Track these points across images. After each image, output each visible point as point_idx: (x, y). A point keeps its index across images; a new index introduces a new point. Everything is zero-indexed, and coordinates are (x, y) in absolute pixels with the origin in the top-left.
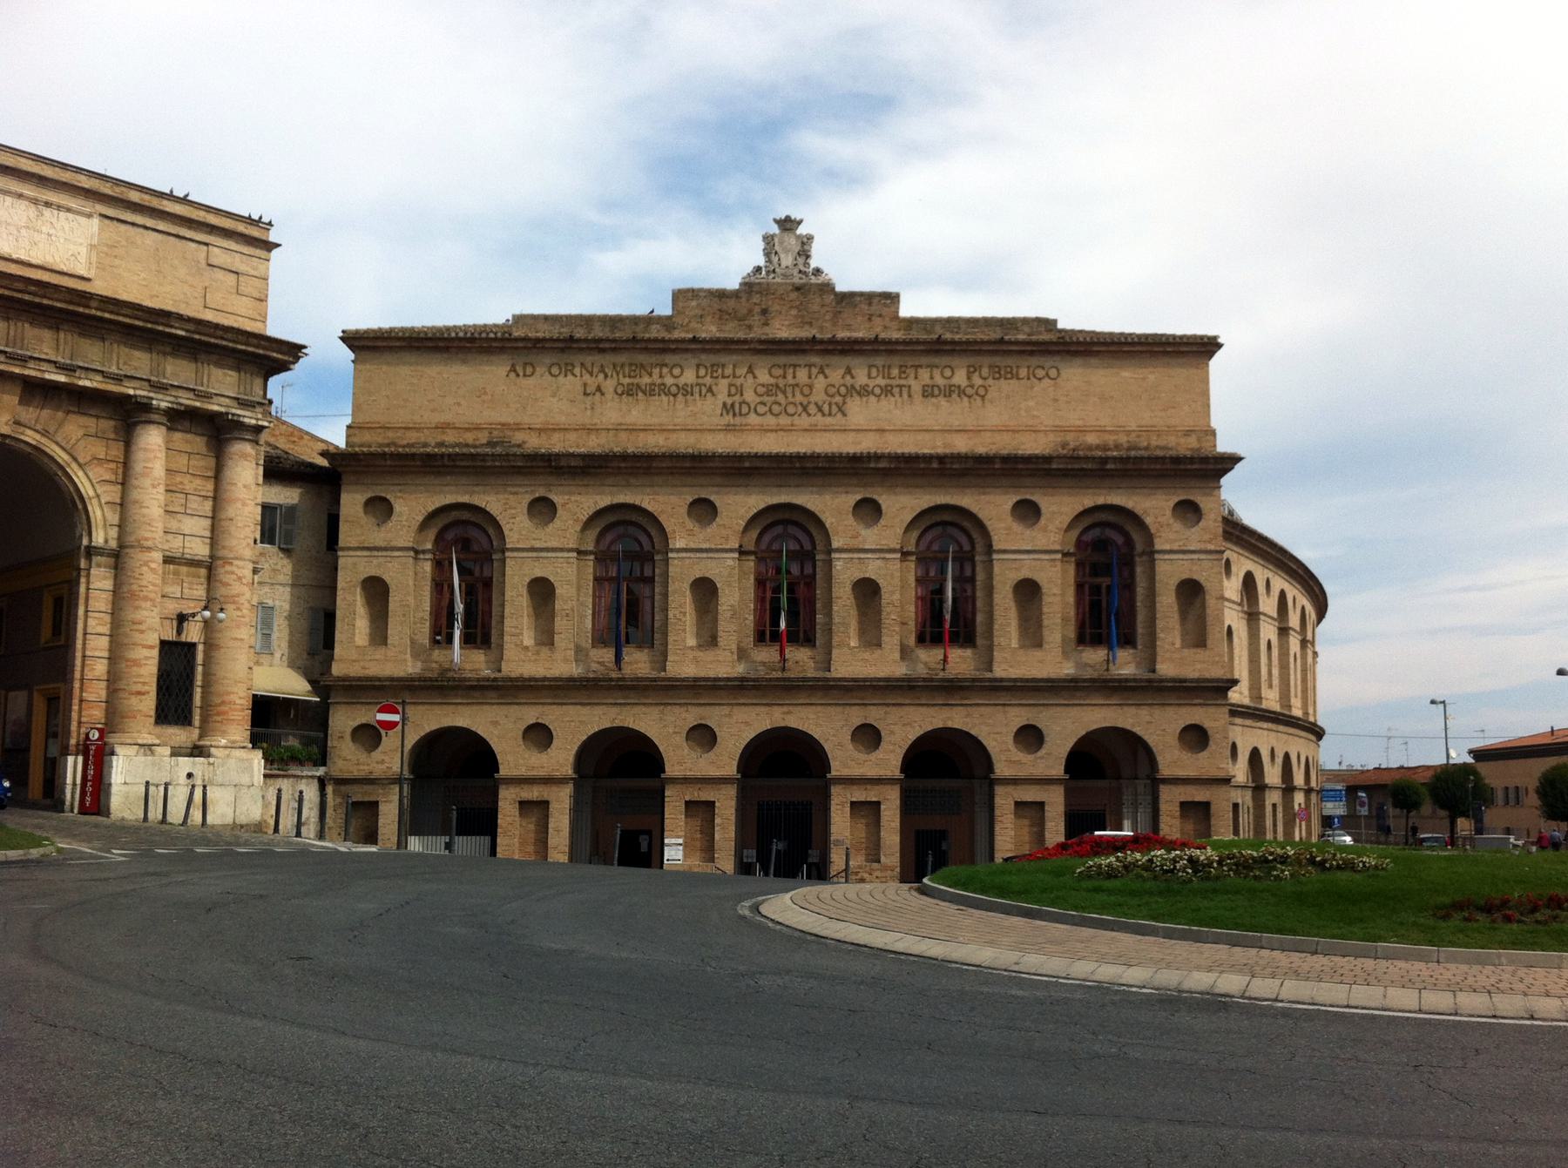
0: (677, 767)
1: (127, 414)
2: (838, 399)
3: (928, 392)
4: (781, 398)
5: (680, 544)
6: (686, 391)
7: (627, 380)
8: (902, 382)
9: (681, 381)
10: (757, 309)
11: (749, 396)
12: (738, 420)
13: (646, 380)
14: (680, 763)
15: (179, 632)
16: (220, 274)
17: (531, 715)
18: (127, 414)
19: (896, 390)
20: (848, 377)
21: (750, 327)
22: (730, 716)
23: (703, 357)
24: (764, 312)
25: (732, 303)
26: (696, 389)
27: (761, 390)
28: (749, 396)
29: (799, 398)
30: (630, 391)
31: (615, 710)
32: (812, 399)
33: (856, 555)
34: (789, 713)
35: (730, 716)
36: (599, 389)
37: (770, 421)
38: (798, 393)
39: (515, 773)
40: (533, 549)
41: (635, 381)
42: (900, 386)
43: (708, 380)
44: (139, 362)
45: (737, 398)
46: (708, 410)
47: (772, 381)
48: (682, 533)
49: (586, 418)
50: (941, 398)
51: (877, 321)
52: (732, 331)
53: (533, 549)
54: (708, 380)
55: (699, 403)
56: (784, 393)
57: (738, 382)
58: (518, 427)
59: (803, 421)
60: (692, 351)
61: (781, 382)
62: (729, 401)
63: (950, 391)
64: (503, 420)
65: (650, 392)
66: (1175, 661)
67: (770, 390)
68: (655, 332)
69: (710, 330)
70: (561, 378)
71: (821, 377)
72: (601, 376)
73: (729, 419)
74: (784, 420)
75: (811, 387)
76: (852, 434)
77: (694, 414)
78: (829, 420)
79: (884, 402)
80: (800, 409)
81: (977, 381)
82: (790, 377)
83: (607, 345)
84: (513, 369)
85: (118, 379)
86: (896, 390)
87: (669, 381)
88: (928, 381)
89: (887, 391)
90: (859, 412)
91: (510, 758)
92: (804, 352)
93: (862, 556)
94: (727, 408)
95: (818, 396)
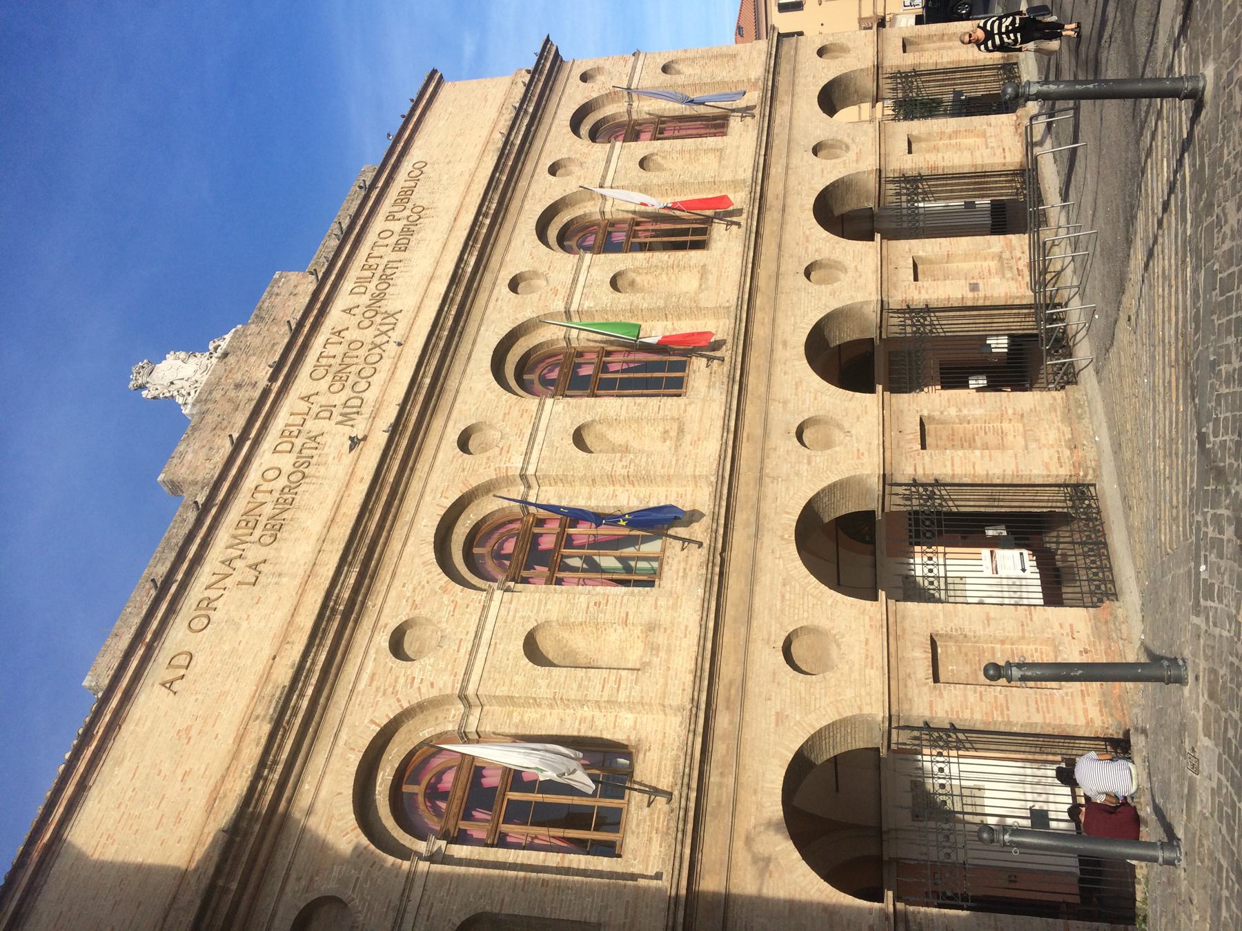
0: (865, 459)
2: (378, 319)
3: (401, 247)
4: (353, 369)
6: (303, 466)
7: (258, 532)
9: (287, 467)
10: (232, 394)
12: (366, 410)
14: (860, 455)
17: (769, 658)
19: (389, 272)
22: (785, 403)
26: (306, 452)
28: (339, 399)
29: (362, 352)
30: (276, 528)
31: (767, 540)
34: (785, 344)
36: (255, 567)
38: (355, 353)
39: (878, 683)
41: (263, 520)
43: (298, 442)
48: (501, 459)
49: (290, 586)
50: (412, 238)
54: (298, 442)
55: (326, 450)
56: (349, 366)
57: (315, 409)
61: (333, 370)
62: (340, 418)
70: (215, 616)
72: (238, 564)
76: (426, 301)
80: (378, 350)
83: (193, 548)
84: (168, 685)
86: (389, 272)
87: (283, 481)
89: (386, 279)
91: (849, 694)
92: (305, 347)
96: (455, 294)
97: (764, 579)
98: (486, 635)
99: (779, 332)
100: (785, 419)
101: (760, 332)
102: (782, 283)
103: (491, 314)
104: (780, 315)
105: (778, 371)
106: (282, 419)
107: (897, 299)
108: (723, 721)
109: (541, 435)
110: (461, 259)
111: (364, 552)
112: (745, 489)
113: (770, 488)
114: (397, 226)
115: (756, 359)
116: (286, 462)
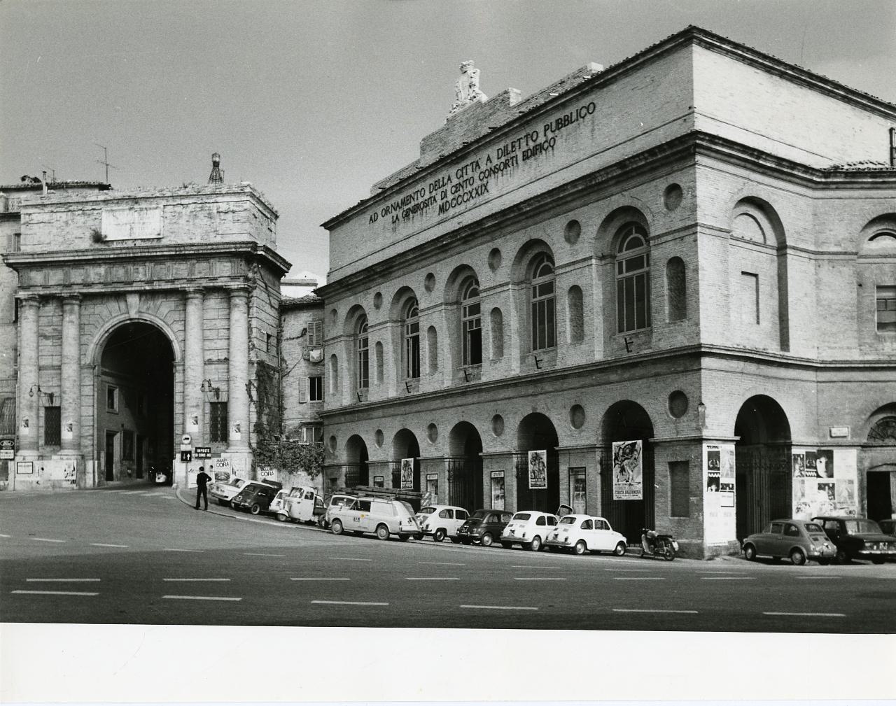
1: (182, 296)
3: (526, 157)
8: (513, 154)
11: (450, 197)
13: (413, 204)
18: (182, 296)
20: (489, 164)
27: (454, 189)
32: (474, 186)
42: (512, 158)
44: (182, 269)
45: (445, 200)
46: (432, 214)
59: (472, 202)
63: (538, 149)
66: (667, 337)
73: (443, 216)
81: (550, 135)
82: (464, 175)
85: (172, 281)
88: (526, 149)
89: (506, 165)
94: (442, 209)
114: (541, 139)
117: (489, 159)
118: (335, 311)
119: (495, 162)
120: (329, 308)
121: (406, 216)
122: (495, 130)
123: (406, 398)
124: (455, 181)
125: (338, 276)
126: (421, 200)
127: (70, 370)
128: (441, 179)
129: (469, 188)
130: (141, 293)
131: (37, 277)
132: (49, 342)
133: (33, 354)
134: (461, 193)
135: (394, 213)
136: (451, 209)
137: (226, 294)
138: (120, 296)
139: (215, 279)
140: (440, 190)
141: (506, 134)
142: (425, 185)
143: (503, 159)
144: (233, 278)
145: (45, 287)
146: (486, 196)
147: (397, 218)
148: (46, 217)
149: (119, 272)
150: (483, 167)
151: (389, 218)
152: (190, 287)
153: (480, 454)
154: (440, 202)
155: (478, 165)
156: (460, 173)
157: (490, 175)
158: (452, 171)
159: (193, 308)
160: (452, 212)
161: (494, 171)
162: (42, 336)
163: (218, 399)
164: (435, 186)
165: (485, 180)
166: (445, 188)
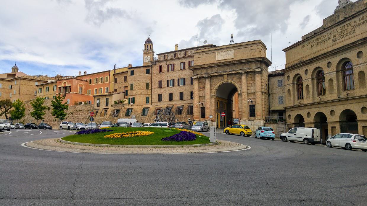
0: (329, 119)
5: (326, 72)
6: (326, 40)
7: (317, 42)
10: (337, 16)
11: (337, 36)
13: (320, 40)
15: (252, 103)
16: (253, 50)
20: (355, 23)
21: (336, 21)
23: (328, 31)
24: (338, 16)
25: (332, 17)
31: (318, 109)
32: (348, 32)
33: (358, 66)
35: (337, 108)
37: (341, 40)
40: (306, 79)
45: (335, 38)
46: (330, 42)
47: (340, 31)
51: (360, 7)
52: (333, 23)
53: (306, 79)
58: (302, 58)
59: (347, 37)
60: (325, 31)
64: (301, 57)
65: (321, 43)
67: (340, 33)
68: (321, 30)
69: (329, 25)
71: (350, 26)
73: (334, 43)
74: (343, 39)
75: (348, 29)
77: (328, 44)
78: (352, 35)
79: (363, 26)
82: (344, 29)
85: (237, 71)
90: (358, 31)
92: (345, 22)
93: (359, 66)
94: (333, 41)
95: (350, 30)
96: (351, 45)
97: (314, 109)
98: (307, 80)
99: (350, 105)
100: (334, 108)
101: (350, 102)
102: (361, 103)
103: (351, 53)
104: (353, 104)
105: (343, 106)
106: (332, 30)
107: (359, 123)
108: (303, 108)
109: (330, 74)
110: (358, 41)
111: (311, 61)
112: (324, 105)
113: (324, 108)
115: (344, 102)
116: (327, 37)
117: (355, 22)
118: (288, 76)
119: (358, 22)
120: (286, 76)
121: (318, 44)
122: (359, 12)
123: (320, 102)
124: (339, 31)
125: (288, 66)
126: (323, 39)
127: (208, 97)
128: (333, 31)
129: (346, 32)
130: (228, 74)
131: (198, 72)
132: (202, 90)
133: (198, 92)
134: (342, 34)
135: (312, 44)
136: (338, 40)
137: (254, 73)
138: (221, 75)
139: (251, 69)
140: (332, 35)
141: (363, 13)
142: (326, 34)
143: (362, 21)
144: (256, 68)
145: (200, 75)
146: (354, 34)
147: (313, 45)
148: (201, 56)
149: (222, 69)
150: (352, 25)
151: (310, 46)
152: (243, 72)
153: (326, 121)
154: (332, 38)
155: (350, 24)
156: (342, 28)
157: (356, 27)
158: (338, 28)
159: (244, 77)
160: (338, 41)
161: (359, 25)
162: (199, 88)
163: (252, 103)
164: (330, 34)
165: (353, 29)
166: (334, 34)
